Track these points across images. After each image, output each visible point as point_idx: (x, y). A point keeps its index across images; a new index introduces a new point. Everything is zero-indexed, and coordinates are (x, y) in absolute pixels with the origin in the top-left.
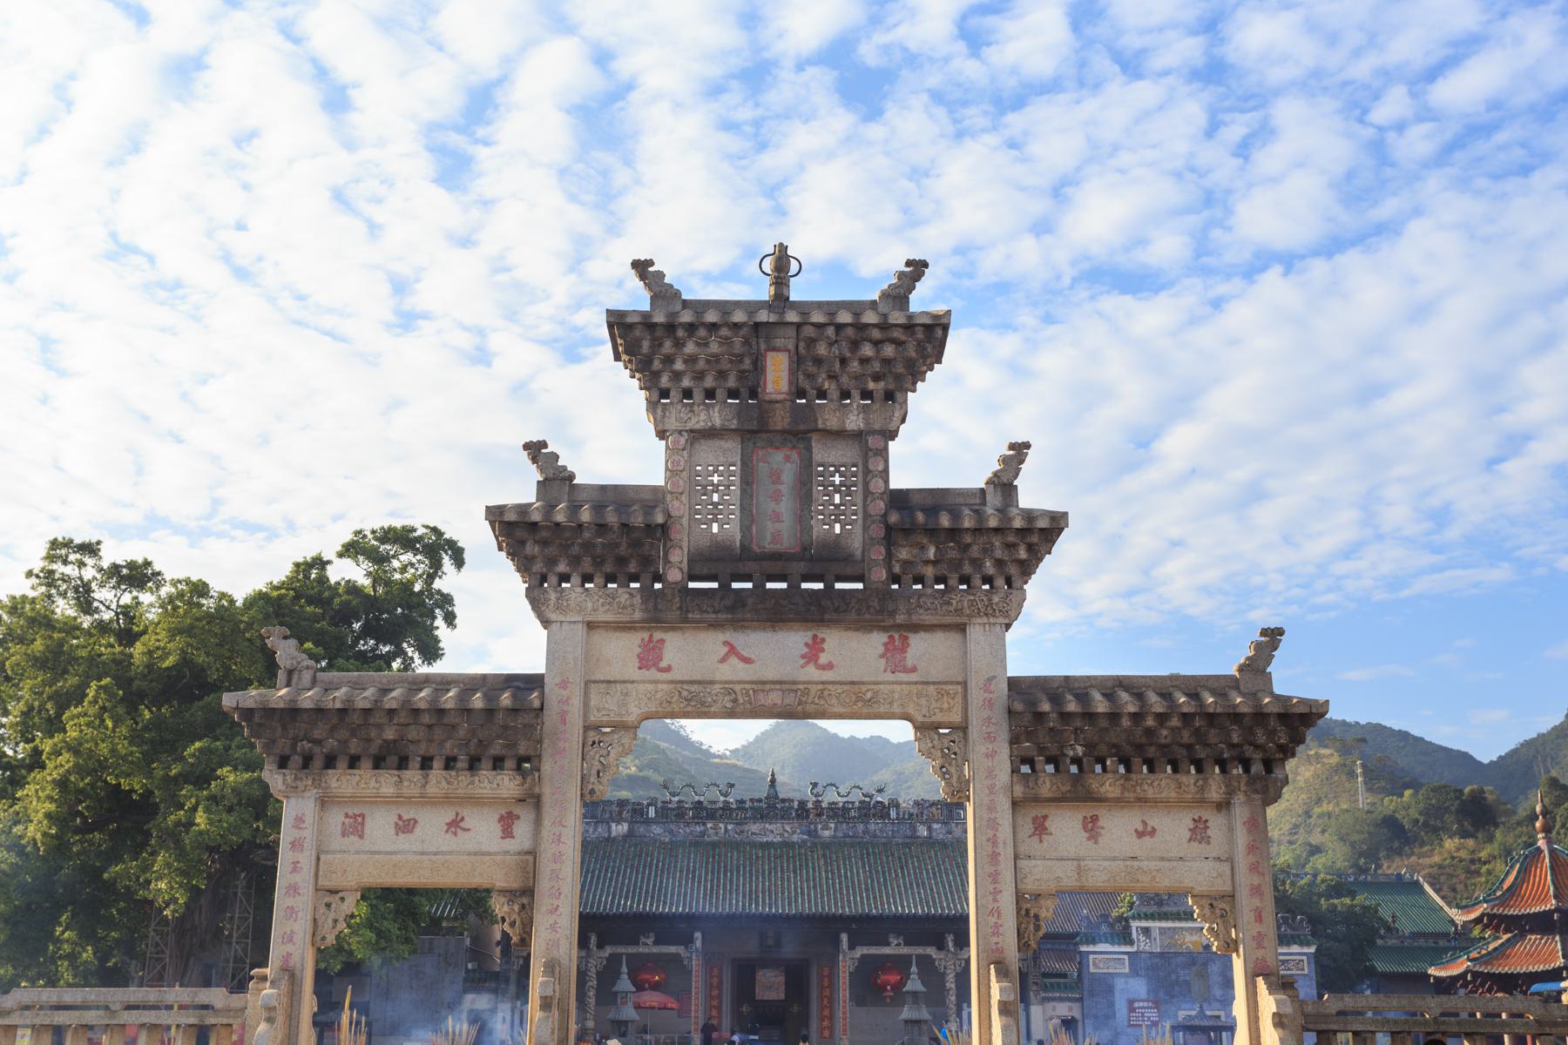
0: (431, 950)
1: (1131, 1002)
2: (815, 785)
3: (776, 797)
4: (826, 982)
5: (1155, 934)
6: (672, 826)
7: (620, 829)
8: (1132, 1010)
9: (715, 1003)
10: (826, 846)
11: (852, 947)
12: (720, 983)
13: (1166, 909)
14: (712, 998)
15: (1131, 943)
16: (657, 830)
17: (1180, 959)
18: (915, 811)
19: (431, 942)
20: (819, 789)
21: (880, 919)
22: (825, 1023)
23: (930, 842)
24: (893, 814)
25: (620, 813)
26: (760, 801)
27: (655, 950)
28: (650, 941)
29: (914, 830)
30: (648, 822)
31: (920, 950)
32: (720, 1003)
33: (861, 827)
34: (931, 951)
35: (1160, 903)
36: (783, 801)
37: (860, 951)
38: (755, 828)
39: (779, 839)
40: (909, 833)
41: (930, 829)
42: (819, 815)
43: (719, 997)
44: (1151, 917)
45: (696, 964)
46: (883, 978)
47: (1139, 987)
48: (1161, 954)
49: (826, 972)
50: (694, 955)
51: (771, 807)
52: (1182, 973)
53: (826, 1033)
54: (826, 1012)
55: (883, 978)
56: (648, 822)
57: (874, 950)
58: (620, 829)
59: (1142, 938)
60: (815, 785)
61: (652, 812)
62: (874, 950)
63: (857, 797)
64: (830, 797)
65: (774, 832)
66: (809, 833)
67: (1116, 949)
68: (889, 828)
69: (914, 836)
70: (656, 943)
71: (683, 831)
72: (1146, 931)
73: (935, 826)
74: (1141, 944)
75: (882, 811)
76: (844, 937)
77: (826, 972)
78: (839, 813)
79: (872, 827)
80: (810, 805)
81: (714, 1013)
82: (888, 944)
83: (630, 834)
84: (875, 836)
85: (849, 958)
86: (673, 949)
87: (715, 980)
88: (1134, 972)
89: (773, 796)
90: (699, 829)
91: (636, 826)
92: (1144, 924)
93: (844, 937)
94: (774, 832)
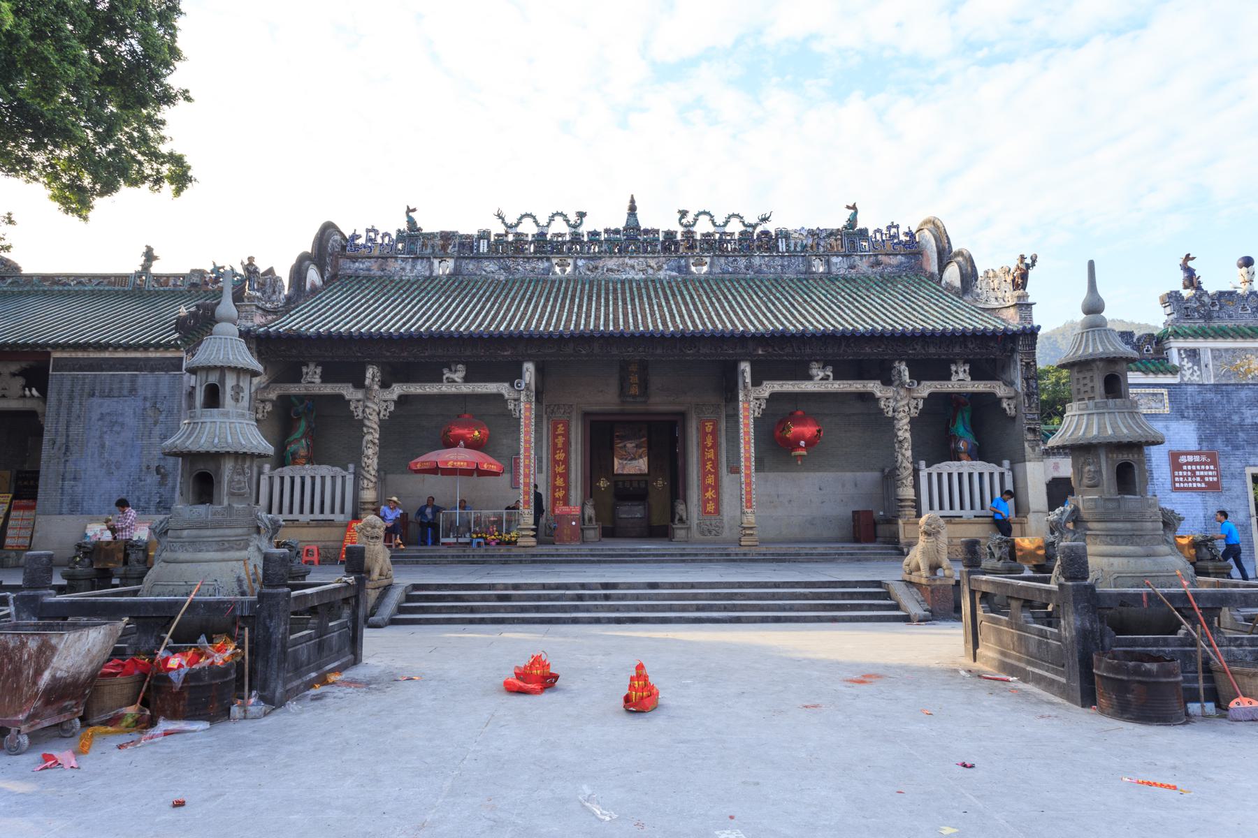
0: (133, 391)
1: (1174, 456)
2: (683, 214)
3: (637, 227)
4: (709, 442)
5: (1207, 357)
6: (509, 263)
7: (443, 268)
8: (1176, 465)
9: (560, 469)
10: (701, 281)
11: (757, 382)
12: (567, 443)
13: (1216, 324)
14: (556, 462)
15: (1174, 371)
16: (490, 266)
17: (1243, 394)
18: (810, 242)
19: (133, 380)
20: (689, 218)
21: (803, 339)
22: (710, 494)
23: (830, 277)
24: (782, 246)
25: (444, 247)
26: (617, 232)
27: (467, 389)
28: (458, 376)
29: (810, 265)
30: (479, 258)
31: (857, 386)
32: (567, 469)
33: (742, 262)
34: (874, 387)
35: (1208, 317)
36: (646, 232)
37: (770, 387)
38: (612, 263)
39: (641, 276)
40: (802, 268)
41: (828, 263)
42: (691, 247)
43: (566, 462)
44: (1204, 334)
45: (525, 410)
46: (794, 430)
47: (1184, 435)
48: (1217, 387)
49: (709, 428)
50: (519, 394)
51: (632, 239)
52: (1248, 413)
53: (711, 507)
54: (710, 480)
55: (794, 430)
56: (479, 258)
57: (789, 387)
58: (443, 268)
59: (1187, 364)
60: (683, 214)
61: (483, 247)
62: (789, 387)
63: (735, 228)
64: (703, 227)
65: (634, 268)
66: (679, 269)
67: (1151, 379)
68: (778, 261)
69: (808, 272)
70: (466, 380)
71: (523, 268)
72: (1193, 354)
73: (834, 260)
74: (1190, 374)
75: (768, 242)
76: (745, 367)
77: (709, 428)
78: (714, 245)
79: (757, 261)
80: (679, 237)
81: (560, 482)
82: (810, 378)
83: (456, 272)
84: (759, 271)
85: (752, 400)
86: (491, 388)
87: (560, 440)
88: (1179, 413)
89: (633, 226)
90: (543, 265)
91: (464, 263)
92: (1191, 344)
93: (745, 367)
94: (634, 268)
